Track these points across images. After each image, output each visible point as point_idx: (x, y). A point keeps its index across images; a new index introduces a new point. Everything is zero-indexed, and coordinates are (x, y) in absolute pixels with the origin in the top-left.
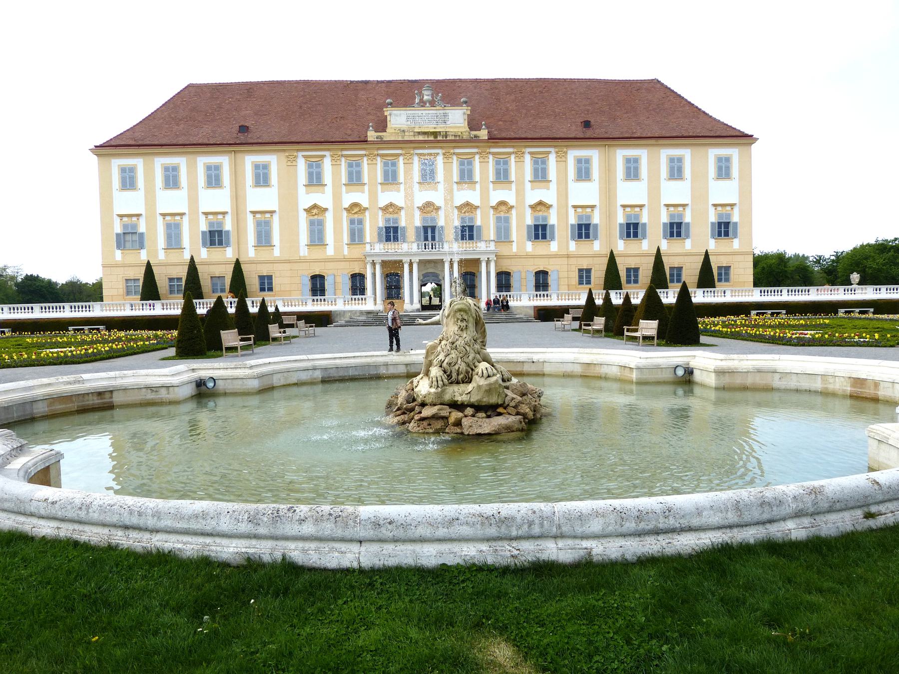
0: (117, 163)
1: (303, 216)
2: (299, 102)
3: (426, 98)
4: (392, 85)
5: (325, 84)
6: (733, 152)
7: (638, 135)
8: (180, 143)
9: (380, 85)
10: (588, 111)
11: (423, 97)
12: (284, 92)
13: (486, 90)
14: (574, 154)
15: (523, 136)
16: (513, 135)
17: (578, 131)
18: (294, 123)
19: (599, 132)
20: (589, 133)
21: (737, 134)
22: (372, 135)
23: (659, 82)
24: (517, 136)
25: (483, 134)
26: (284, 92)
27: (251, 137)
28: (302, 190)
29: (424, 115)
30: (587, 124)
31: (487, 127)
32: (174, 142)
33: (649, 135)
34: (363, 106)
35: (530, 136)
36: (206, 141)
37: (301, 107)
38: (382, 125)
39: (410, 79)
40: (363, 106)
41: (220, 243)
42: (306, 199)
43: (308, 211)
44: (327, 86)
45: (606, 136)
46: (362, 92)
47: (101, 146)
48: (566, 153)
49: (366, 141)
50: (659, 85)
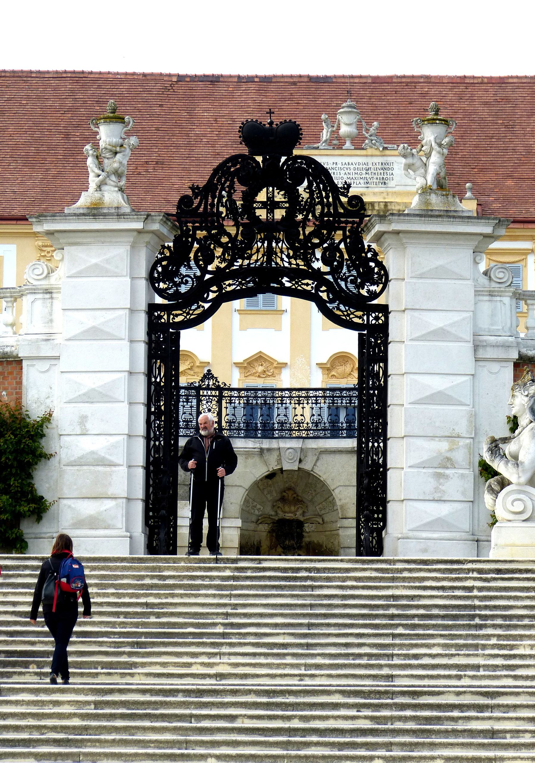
2: (63, 124)
3: (344, 130)
4: (272, 87)
5: (121, 81)
9: (244, 86)
11: (339, 128)
12: (28, 98)
13: (486, 103)
18: (53, 172)
26: (28, 98)
29: (339, 166)
31: (478, 193)
34: (204, 135)
37: (67, 136)
39: (313, 73)
40: (204, 135)
46: (205, 105)
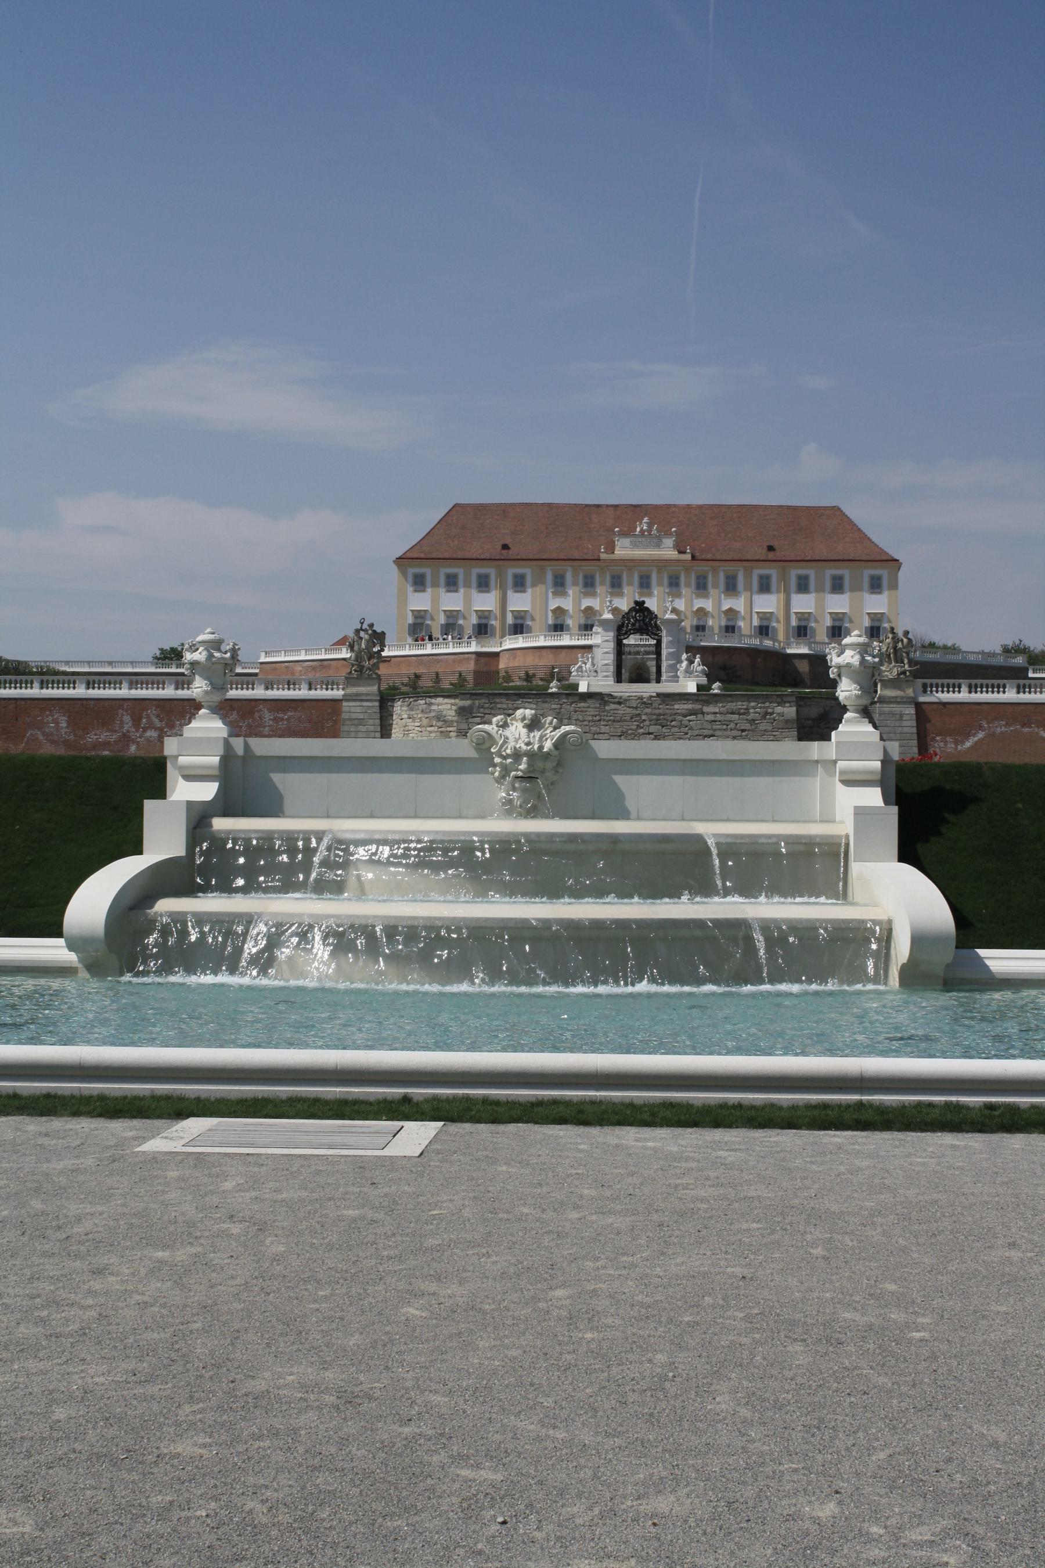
0: (411, 571)
1: (550, 614)
3: (645, 528)
6: (884, 573)
7: (809, 558)
8: (459, 557)
10: (775, 535)
14: (756, 573)
15: (719, 557)
16: (709, 556)
17: (761, 553)
19: (777, 555)
20: (771, 555)
21: (889, 558)
22: (603, 556)
23: (839, 509)
24: (714, 558)
25: (688, 557)
27: (511, 554)
28: (550, 595)
30: (771, 548)
32: (454, 556)
33: (817, 558)
35: (724, 558)
36: (478, 557)
37: (547, 528)
38: (611, 548)
41: (486, 633)
42: (554, 603)
43: (554, 611)
44: (566, 509)
45: (784, 558)
47: (400, 558)
48: (752, 572)
49: (599, 560)
50: (838, 513)
